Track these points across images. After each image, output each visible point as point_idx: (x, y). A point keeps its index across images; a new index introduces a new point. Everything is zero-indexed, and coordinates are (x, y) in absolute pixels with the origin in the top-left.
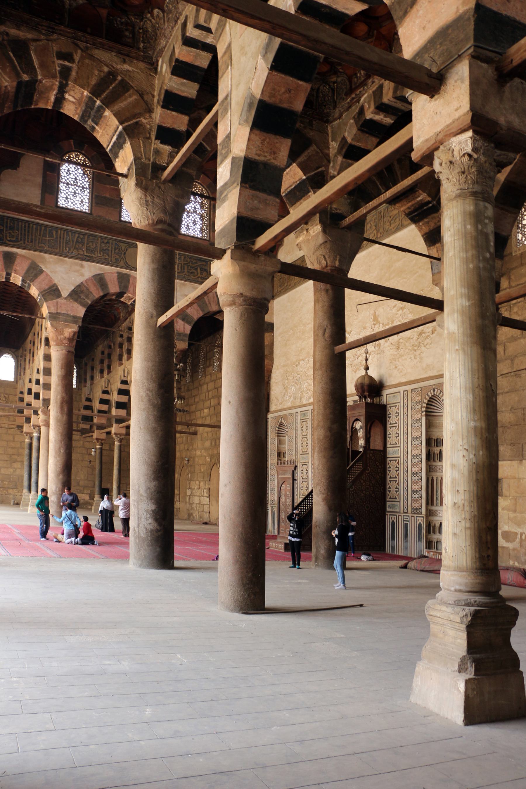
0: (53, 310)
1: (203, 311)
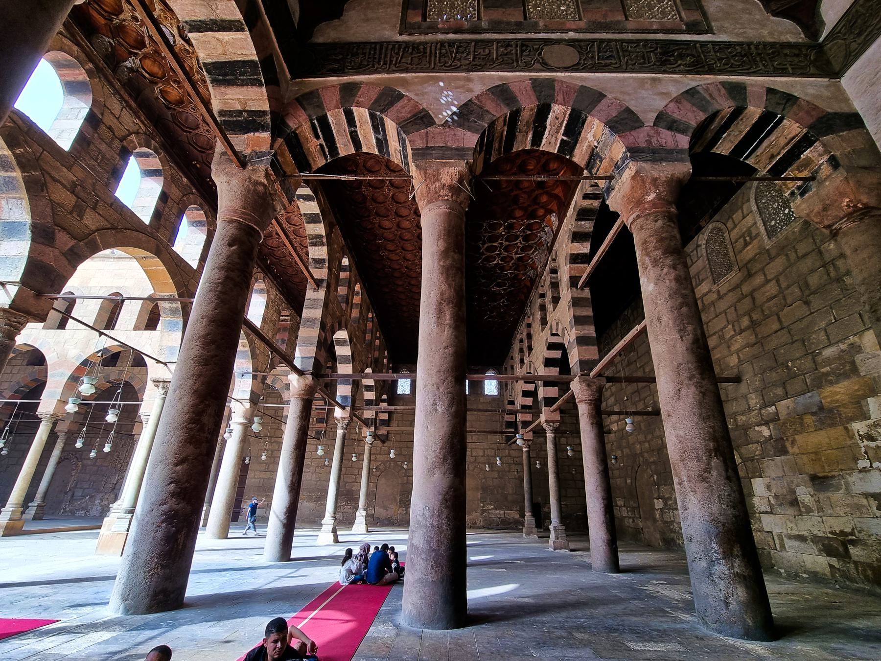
0: (420, 144)
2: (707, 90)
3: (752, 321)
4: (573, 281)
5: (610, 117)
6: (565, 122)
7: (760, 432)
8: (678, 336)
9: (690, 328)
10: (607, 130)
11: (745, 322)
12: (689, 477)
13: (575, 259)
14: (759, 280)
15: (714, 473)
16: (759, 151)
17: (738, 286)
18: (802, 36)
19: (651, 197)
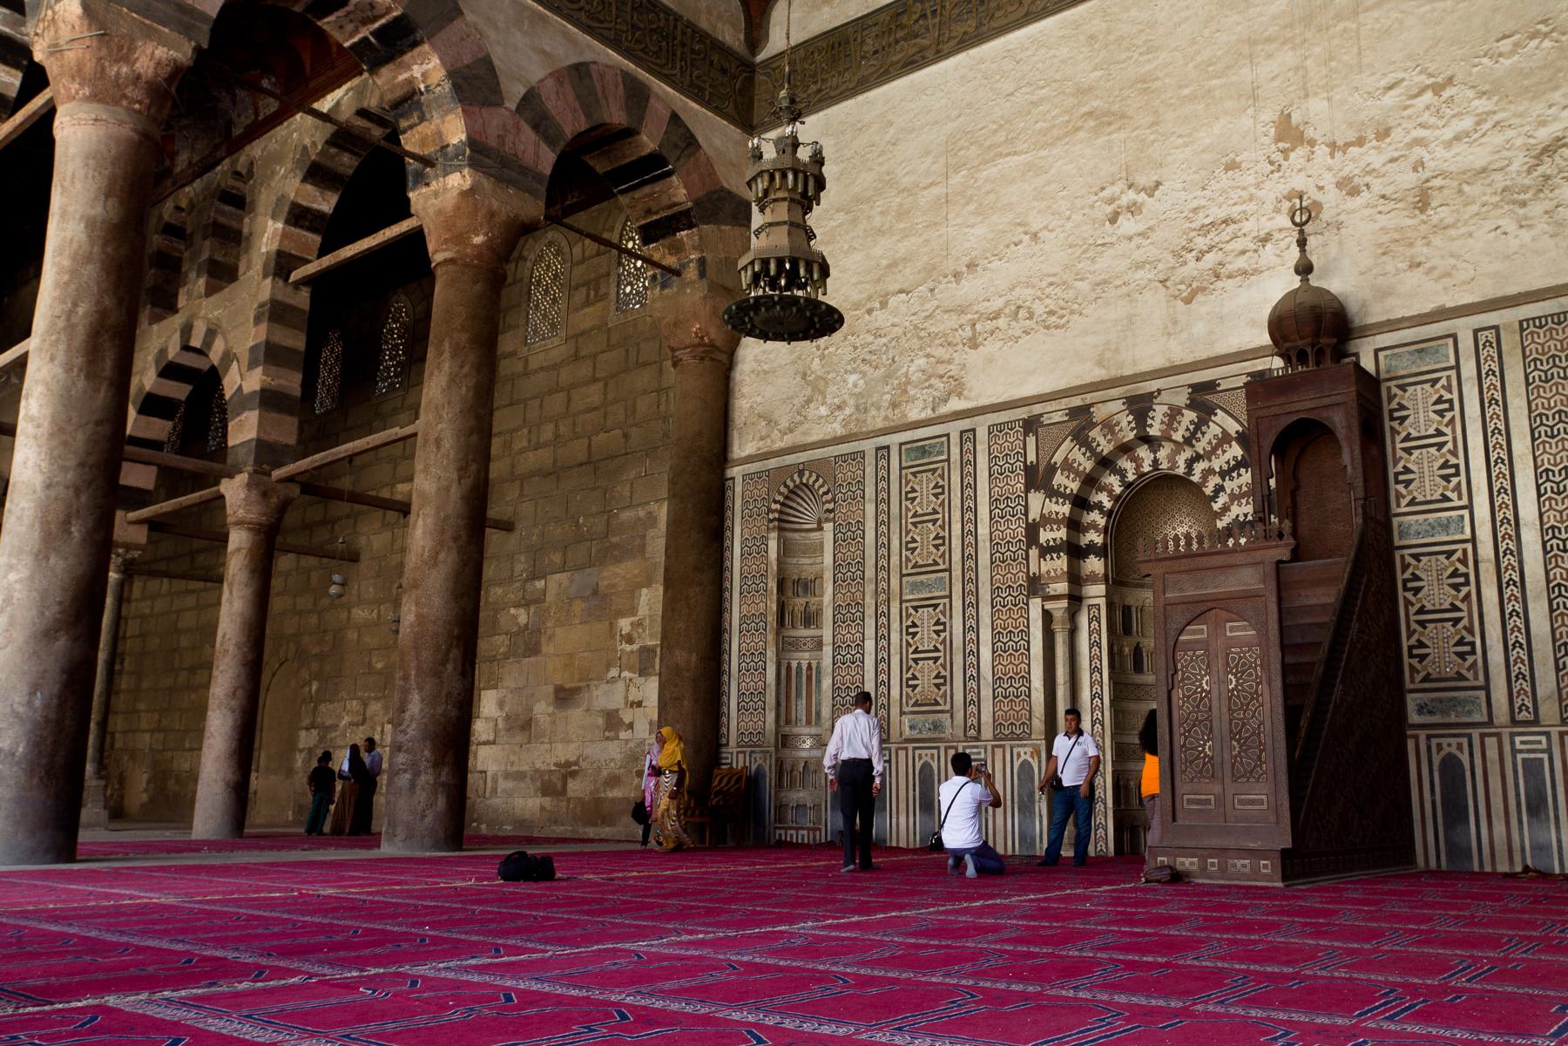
1: (588, 116)
2: (602, 76)
3: (557, 436)
4: (282, 264)
5: (459, 65)
6: (383, 21)
7: (515, 617)
8: (455, 476)
9: (473, 467)
10: (447, 86)
11: (547, 432)
12: (418, 669)
13: (299, 216)
14: (585, 370)
15: (450, 667)
16: (637, 194)
17: (555, 367)
18: (742, 37)
19: (478, 240)
